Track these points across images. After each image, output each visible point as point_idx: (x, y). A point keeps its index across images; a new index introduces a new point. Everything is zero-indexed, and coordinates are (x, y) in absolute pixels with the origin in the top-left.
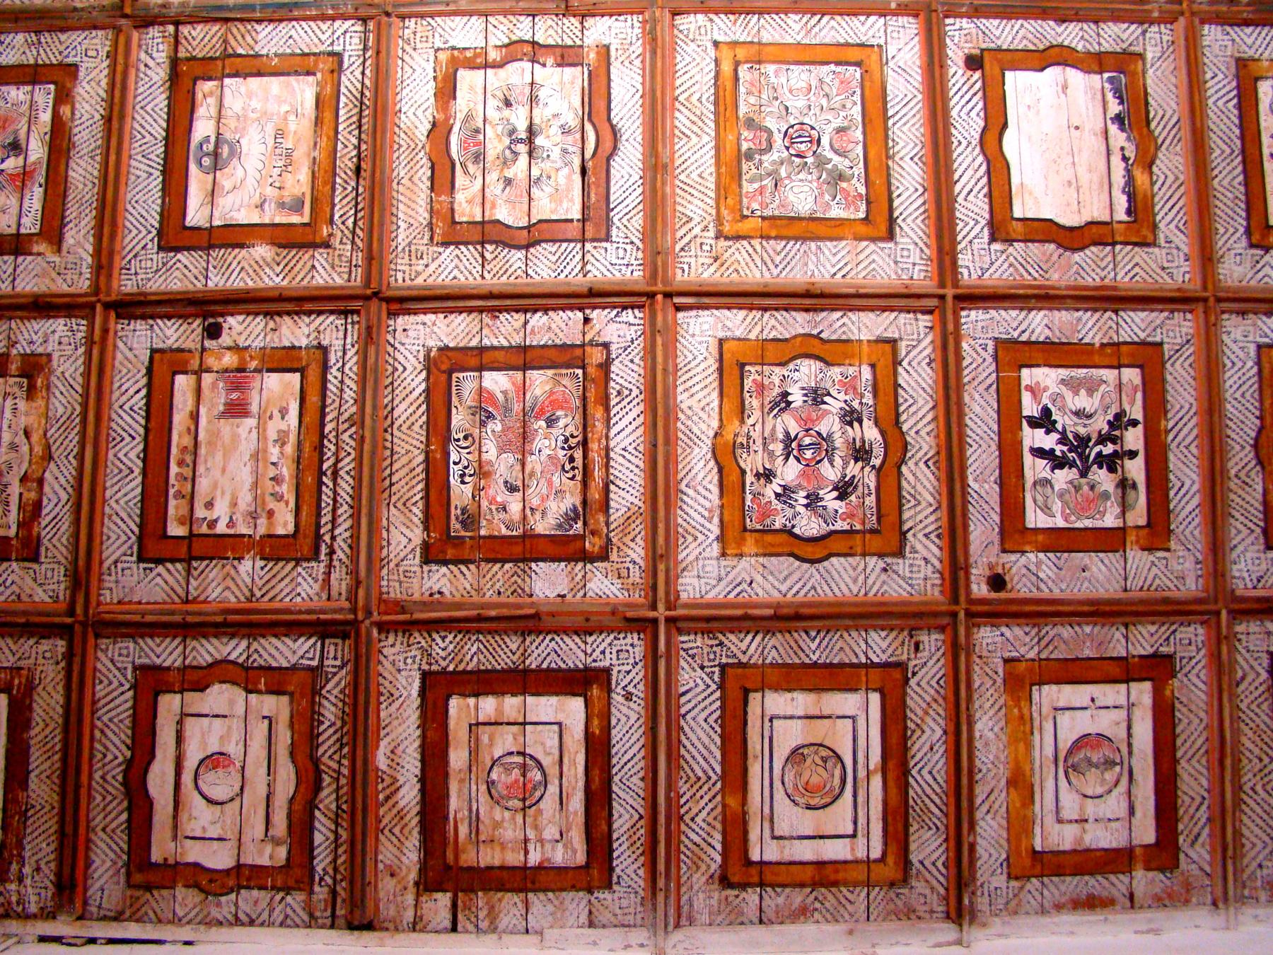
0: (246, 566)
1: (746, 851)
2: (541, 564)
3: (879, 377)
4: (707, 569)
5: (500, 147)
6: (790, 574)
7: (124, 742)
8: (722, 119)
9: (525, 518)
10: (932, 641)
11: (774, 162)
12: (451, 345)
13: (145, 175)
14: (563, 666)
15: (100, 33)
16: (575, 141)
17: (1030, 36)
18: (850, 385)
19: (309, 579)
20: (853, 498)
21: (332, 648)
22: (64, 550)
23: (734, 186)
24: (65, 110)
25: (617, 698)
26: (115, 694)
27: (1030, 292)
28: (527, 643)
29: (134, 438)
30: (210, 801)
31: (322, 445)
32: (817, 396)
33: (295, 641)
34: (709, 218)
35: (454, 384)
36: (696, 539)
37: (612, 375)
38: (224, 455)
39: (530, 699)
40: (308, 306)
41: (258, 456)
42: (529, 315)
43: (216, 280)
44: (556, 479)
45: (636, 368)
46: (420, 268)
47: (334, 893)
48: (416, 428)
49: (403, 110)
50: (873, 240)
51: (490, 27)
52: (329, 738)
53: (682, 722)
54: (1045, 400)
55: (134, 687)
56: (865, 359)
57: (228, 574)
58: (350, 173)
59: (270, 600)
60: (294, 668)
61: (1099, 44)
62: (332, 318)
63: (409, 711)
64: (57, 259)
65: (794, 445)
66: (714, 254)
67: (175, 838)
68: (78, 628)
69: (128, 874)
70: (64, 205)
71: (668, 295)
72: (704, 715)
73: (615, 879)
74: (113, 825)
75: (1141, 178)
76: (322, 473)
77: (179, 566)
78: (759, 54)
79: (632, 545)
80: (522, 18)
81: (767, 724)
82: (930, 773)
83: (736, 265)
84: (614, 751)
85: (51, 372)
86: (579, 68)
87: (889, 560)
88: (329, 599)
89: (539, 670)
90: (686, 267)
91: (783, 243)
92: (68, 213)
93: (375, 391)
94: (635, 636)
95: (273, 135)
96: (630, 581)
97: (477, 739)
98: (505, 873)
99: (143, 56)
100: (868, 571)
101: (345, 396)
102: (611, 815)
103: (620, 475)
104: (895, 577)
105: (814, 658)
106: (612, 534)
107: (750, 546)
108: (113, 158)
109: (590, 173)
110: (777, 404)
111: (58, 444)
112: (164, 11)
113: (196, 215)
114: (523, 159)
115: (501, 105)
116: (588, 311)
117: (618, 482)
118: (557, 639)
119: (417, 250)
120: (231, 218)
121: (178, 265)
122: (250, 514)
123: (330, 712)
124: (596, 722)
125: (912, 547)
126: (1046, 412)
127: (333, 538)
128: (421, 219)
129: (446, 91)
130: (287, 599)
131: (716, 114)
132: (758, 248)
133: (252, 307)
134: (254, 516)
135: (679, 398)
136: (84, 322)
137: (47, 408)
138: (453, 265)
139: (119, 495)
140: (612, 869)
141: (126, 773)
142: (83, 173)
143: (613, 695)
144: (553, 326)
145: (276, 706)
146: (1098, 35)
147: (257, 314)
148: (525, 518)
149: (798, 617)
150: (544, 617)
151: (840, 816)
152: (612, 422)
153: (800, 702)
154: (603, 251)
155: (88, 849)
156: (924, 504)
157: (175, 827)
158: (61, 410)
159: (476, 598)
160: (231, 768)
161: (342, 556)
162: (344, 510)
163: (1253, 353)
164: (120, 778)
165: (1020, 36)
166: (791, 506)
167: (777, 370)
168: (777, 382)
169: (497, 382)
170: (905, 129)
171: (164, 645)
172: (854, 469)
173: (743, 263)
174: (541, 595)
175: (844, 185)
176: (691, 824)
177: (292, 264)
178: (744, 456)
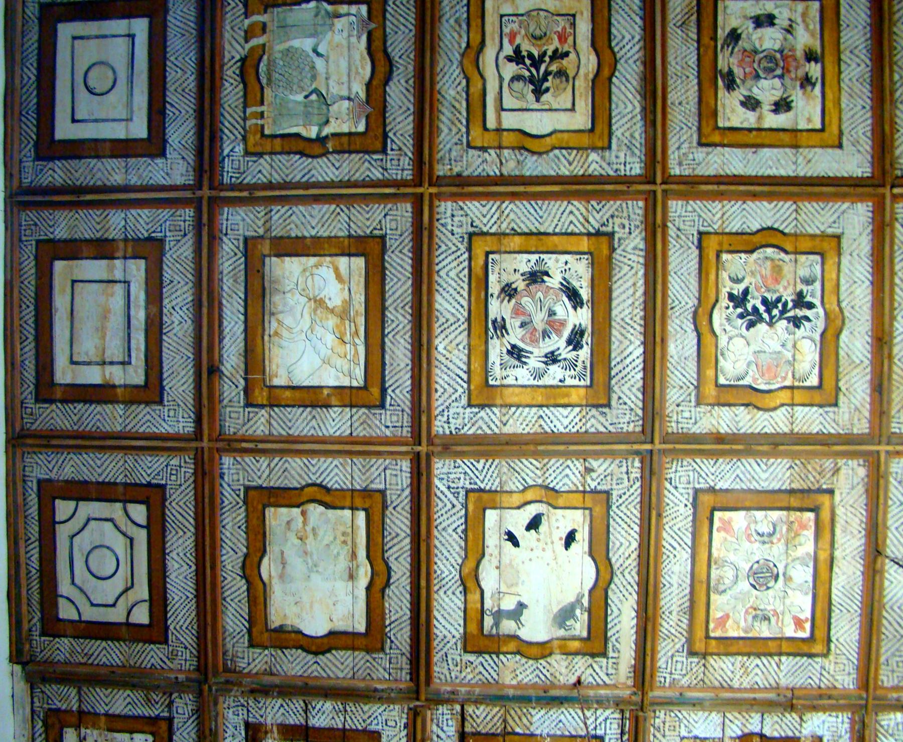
51: (727, 721)
112: (452, 696)
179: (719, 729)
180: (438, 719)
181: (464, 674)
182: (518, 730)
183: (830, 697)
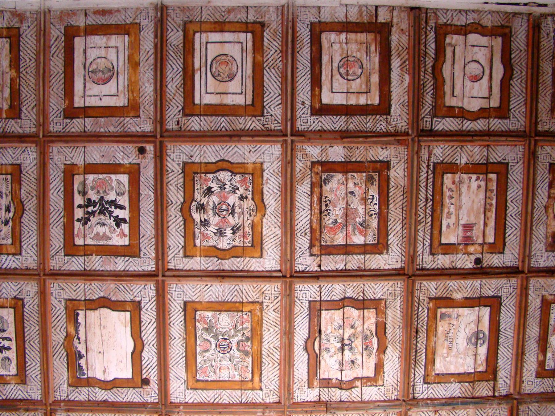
0: (464, 161)
1: (253, 37)
2: (340, 160)
3: (192, 241)
4: (269, 158)
5: (356, 342)
6: (233, 155)
7: (514, 87)
8: (259, 356)
9: (347, 180)
10: (171, 125)
11: (236, 336)
12: (377, 255)
13: (507, 329)
14: (331, 117)
15: (526, 392)
16: (323, 345)
17: (120, 394)
18: (205, 237)
19: (437, 155)
20: (205, 188)
21: (428, 126)
22: (539, 168)
23: (254, 325)
24: (541, 358)
25: (308, 103)
26: (517, 107)
27: (124, 278)
28: (346, 127)
29: (511, 215)
30: (478, 62)
31: (432, 212)
32: (220, 232)
33: (443, 129)
34: (266, 311)
35: (376, 238)
36: (274, 171)
37: (309, 242)
38: (473, 208)
39: (345, 103)
40: (439, 272)
41: (459, 208)
42: (344, 268)
43: (477, 284)
44: (333, 197)
45: (299, 245)
46: (391, 289)
47: (426, 23)
48: (393, 219)
49: (397, 359)
50: (193, 302)
51: (360, 396)
52: (429, 88)
53: (280, 92)
54: (118, 230)
55: (509, 110)
56: (198, 249)
57: (471, 157)
58: (420, 330)
59: (453, 146)
60: (443, 117)
61: (88, 391)
62: (428, 267)
63: (395, 99)
64: (544, 293)
65: (230, 211)
66: (264, 295)
67: (492, 47)
68: (533, 135)
69: (511, 32)
70: (541, 316)
71: (284, 277)
72: (271, 95)
73: (309, 27)
74: (517, 52)
75: (72, 330)
76: (432, 200)
77: (492, 161)
78: (242, 385)
79: (301, 168)
80: (346, 400)
81: (244, 91)
82: (173, 69)
83: (254, 290)
84: (309, 80)
85: (545, 244)
86: (321, 378)
87: (190, 161)
88: (429, 146)
89: (341, 115)
90: (276, 289)
91: (233, 300)
92: (539, 313)
93: (410, 235)
94: (300, 129)
95: (453, 348)
96: (302, 153)
97: (367, 86)
98: (355, 30)
99: (508, 382)
100: (199, 156)
101: (422, 233)
102: (311, 54)
103: (306, 198)
104: (187, 153)
105: (223, 119)
106: (310, 173)
107: (250, 167)
108: (521, 336)
109: (317, 331)
110: (237, 229)
111: (542, 213)
112: (499, 402)
113: (486, 312)
114: (346, 337)
115: (355, 361)
116: (319, 270)
117: (307, 195)
118: (333, 128)
119: (392, 297)
120: (470, 310)
121: (493, 290)
122: (462, 183)
123: (429, 98)
124: (317, 93)
125: (179, 166)
126: (118, 225)
127: (427, 172)
128: (390, 310)
129: (379, 367)
130: (446, 146)
131: (261, 358)
132: (244, 298)
133: (462, 272)
134: (461, 182)
135: (280, 232)
136: (532, 265)
137: (547, 228)
138: (377, 290)
139: (517, 191)
140: (311, 31)
141: (512, 74)
142: (533, 330)
143: (310, 104)
144: (334, 263)
145: (451, 102)
146: (89, 395)
147: (460, 269)
148: (347, 180)
149: (231, 136)
150: (339, 137)
151: (213, 51)
152: (309, 222)
153: (229, 100)
154: (312, 296)
155: (527, 43)
156: (174, 185)
157: (492, 51)
158: (541, 227)
159: (367, 146)
160: (469, 75)
161: (423, 165)
162: (423, 184)
163: (24, 251)
164: (515, 72)
165: (124, 394)
166: (232, 184)
167: (237, 244)
168: (237, 239)
169: (358, 239)
170: (178, 352)
171: (497, 127)
172: (204, 200)
173: (251, 291)
174: (340, 147)
175: (206, 326)
176: (277, 49)
177: (445, 290)
178: (252, 206)
179: (364, 391)
180: (507, 387)
181: (493, 412)
182: (467, 384)
183: (307, 412)
